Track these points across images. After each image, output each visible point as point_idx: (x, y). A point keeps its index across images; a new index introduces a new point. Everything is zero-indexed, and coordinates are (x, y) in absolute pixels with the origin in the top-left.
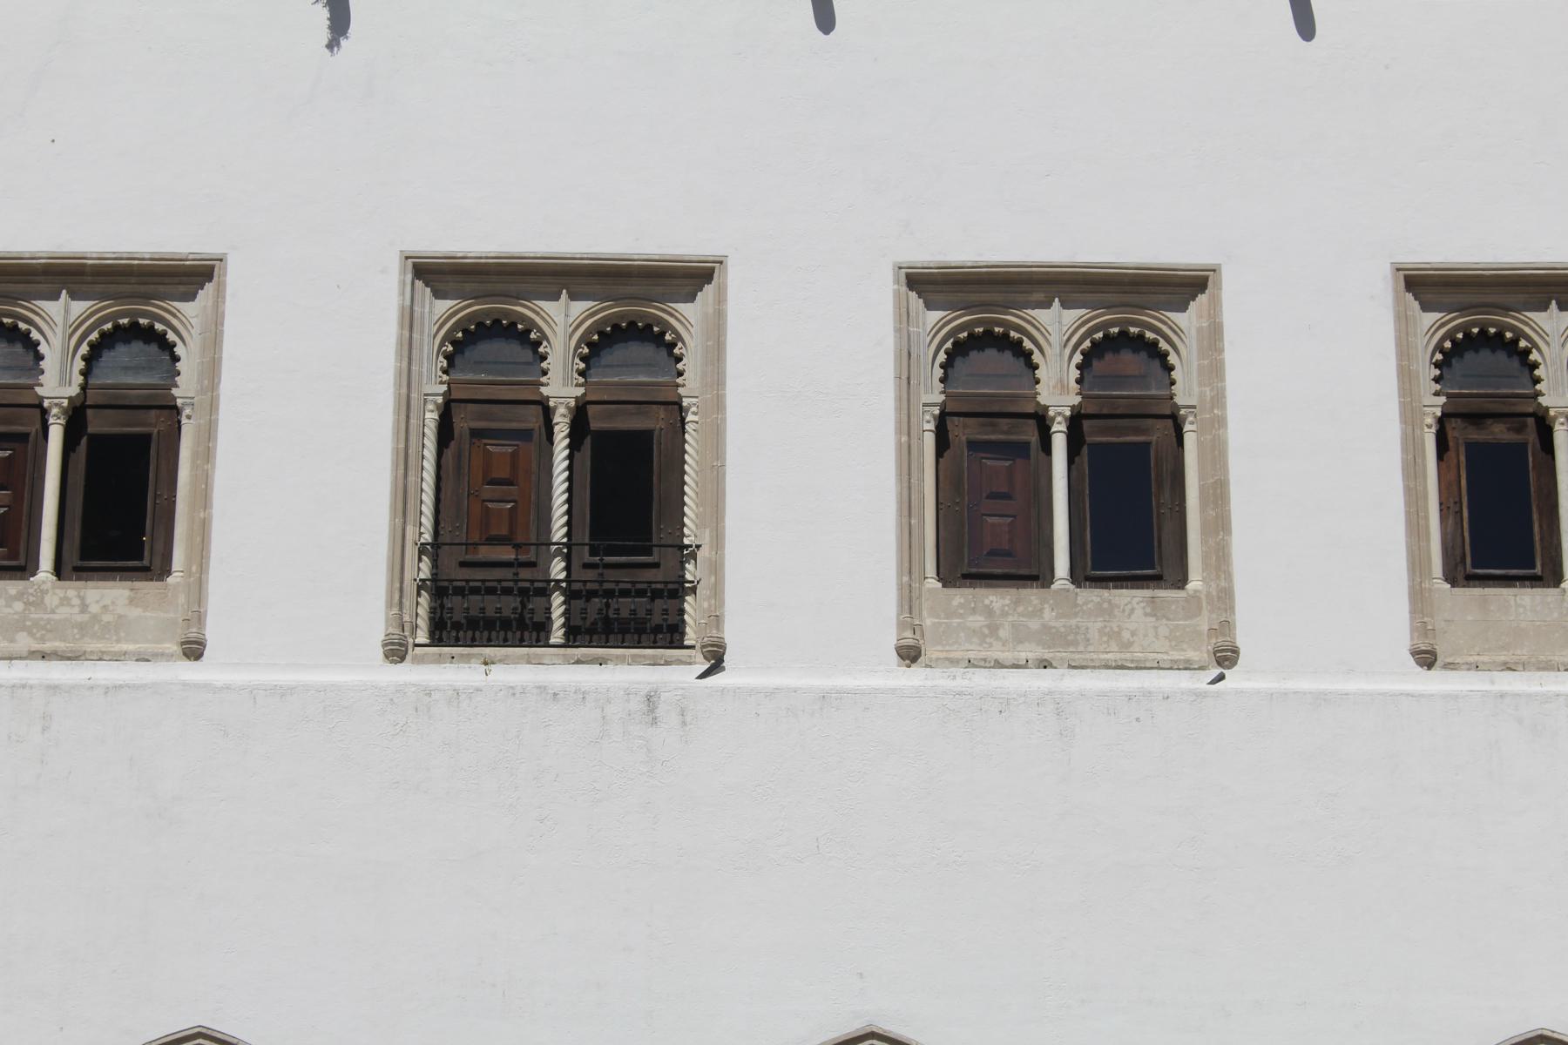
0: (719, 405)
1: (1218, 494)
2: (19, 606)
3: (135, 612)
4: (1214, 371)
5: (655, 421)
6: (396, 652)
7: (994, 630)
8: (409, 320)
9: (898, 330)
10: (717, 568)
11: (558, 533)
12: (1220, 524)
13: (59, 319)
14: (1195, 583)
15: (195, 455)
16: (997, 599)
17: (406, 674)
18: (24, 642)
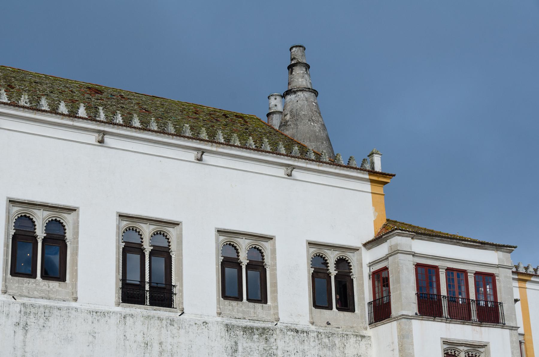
0: (180, 255)
1: (275, 285)
2: (34, 285)
3: (60, 289)
4: (274, 258)
6: (118, 305)
7: (233, 310)
8: (118, 227)
9: (216, 242)
10: (181, 291)
12: (275, 291)
13: (41, 217)
14: (269, 302)
15: (72, 254)
17: (119, 309)
18: (35, 293)
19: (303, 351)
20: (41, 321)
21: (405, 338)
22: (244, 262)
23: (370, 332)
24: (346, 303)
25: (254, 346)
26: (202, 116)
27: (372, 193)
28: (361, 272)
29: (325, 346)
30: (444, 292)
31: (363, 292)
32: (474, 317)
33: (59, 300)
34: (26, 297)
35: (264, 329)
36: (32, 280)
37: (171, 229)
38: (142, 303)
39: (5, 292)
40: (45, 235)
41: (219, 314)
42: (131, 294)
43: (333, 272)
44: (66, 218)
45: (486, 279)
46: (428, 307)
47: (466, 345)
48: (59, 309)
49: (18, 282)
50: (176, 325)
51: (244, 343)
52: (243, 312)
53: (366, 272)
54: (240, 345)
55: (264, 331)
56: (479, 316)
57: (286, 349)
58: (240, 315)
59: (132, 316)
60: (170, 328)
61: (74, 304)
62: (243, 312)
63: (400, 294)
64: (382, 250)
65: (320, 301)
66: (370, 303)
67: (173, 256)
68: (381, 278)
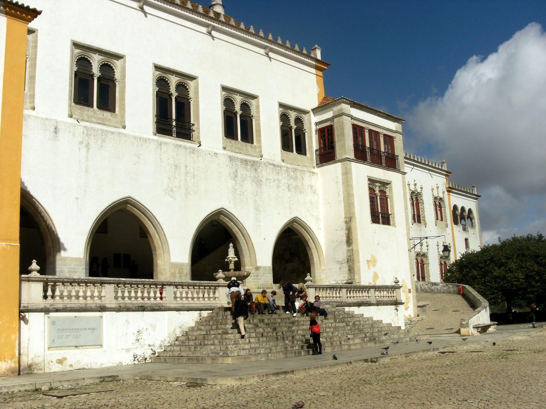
0: (197, 101)
1: (259, 131)
2: (92, 113)
3: (112, 118)
4: (258, 112)
7: (233, 146)
8: (154, 74)
11: (174, 117)
12: (259, 136)
14: (255, 143)
15: (120, 92)
16: (233, 142)
18: (94, 120)
19: (279, 181)
20: (99, 142)
21: (347, 174)
23: (316, 170)
24: (301, 149)
25: (248, 173)
27: (316, 75)
28: (310, 129)
29: (291, 178)
30: (368, 145)
31: (313, 142)
33: (112, 126)
34: (87, 121)
35: (254, 162)
36: (91, 109)
37: (189, 82)
38: (172, 136)
39: (71, 116)
40: (100, 74)
43: (294, 127)
44: (115, 63)
46: (360, 155)
48: (112, 133)
49: (80, 109)
50: (196, 154)
51: (241, 171)
53: (314, 128)
54: (239, 172)
55: (254, 163)
57: (268, 177)
58: (237, 151)
59: (166, 143)
60: (192, 155)
61: (122, 131)
62: (239, 149)
63: (344, 143)
65: (286, 146)
66: (316, 151)
67: (191, 102)
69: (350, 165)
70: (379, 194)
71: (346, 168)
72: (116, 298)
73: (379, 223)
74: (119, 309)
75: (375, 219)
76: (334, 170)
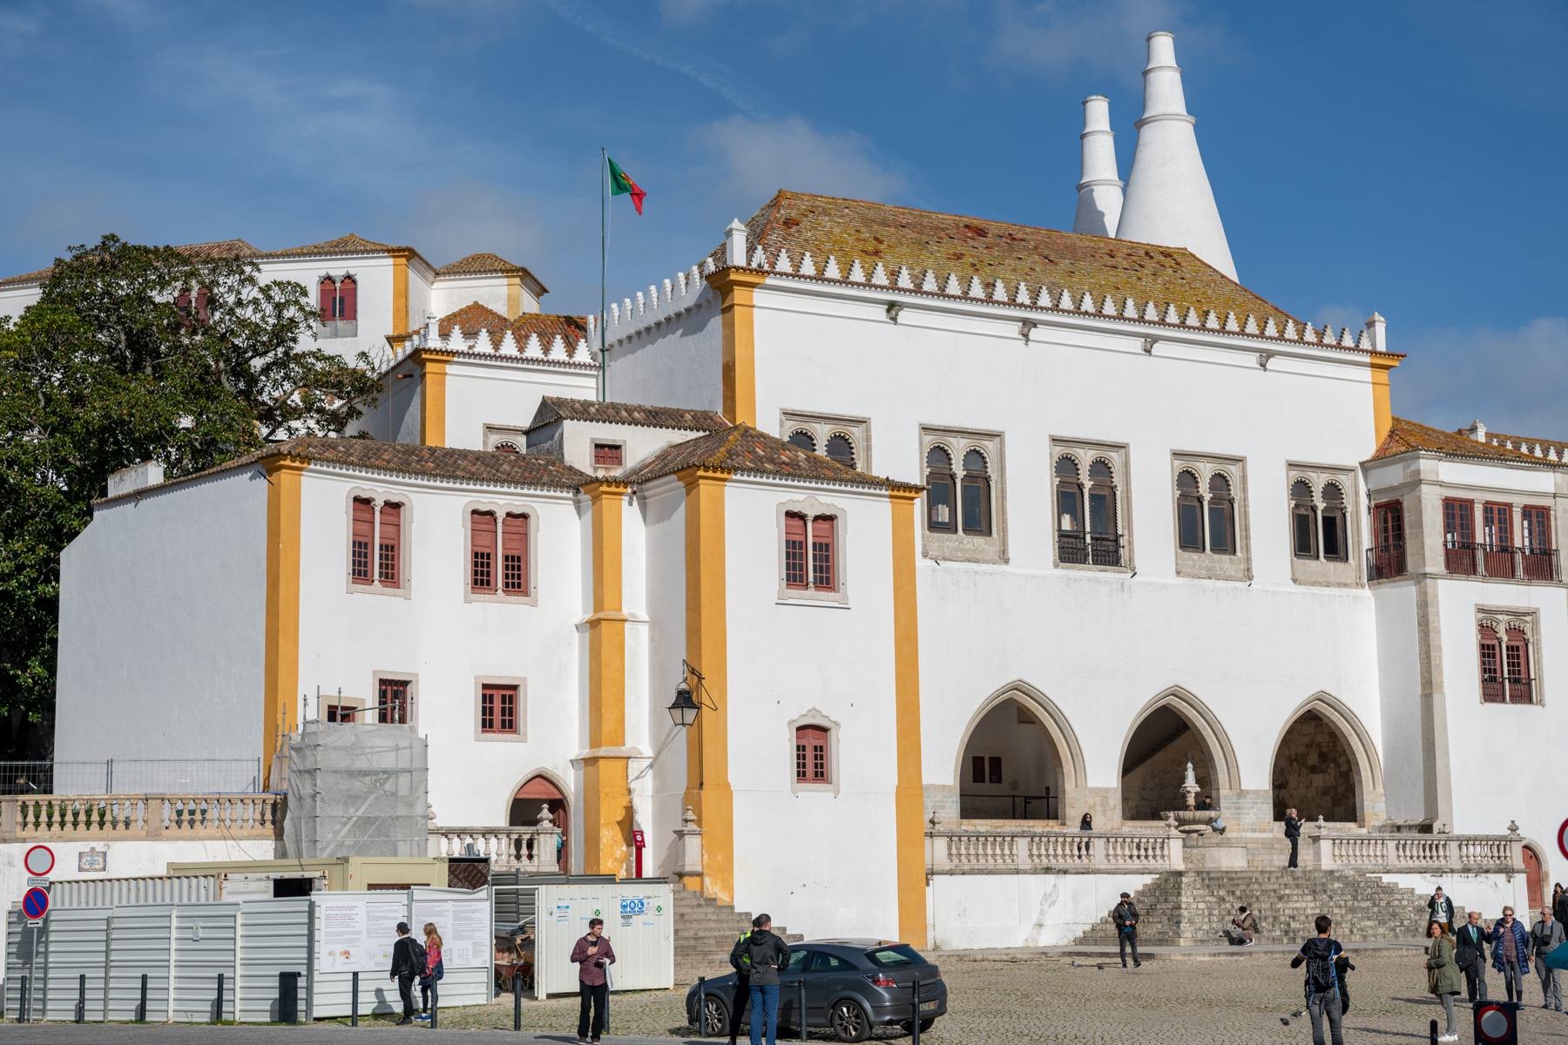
1: (1246, 528)
4: (1245, 490)
5: (1105, 492)
6: (1056, 566)
10: (1130, 543)
11: (1088, 529)
16: (1195, 556)
17: (1059, 572)
21: (1424, 607)
22: (1207, 497)
24: (1335, 548)
26: (1120, 261)
31: (1362, 533)
32: (1520, 571)
38: (1084, 561)
41: (1178, 573)
42: (1070, 550)
43: (1321, 505)
45: (1539, 517)
46: (1461, 560)
47: (1508, 613)
52: (1209, 569)
56: (1527, 571)
61: (1004, 567)
64: (1393, 475)
65: (1303, 546)
68: (1392, 518)
69: (1436, 587)
70: (1505, 638)
71: (1425, 594)
72: (1031, 855)
73: (1503, 701)
74: (1035, 872)
75: (1492, 690)
76: (1401, 592)
